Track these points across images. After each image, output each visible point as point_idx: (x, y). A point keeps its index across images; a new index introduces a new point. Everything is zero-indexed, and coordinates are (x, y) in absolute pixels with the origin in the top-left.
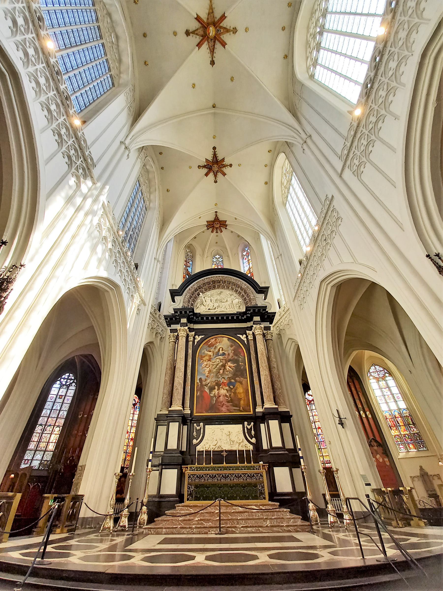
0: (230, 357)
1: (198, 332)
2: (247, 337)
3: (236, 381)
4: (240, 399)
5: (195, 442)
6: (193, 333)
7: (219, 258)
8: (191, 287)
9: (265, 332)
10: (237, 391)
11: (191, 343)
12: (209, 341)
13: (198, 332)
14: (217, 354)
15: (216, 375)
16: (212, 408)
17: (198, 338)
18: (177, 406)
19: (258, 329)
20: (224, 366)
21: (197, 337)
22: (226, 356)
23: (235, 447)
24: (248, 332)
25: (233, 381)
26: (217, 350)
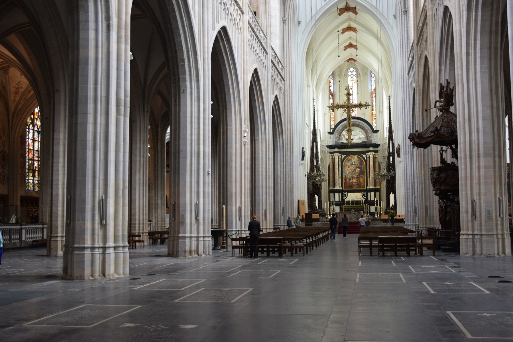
0: (358, 166)
1: (343, 153)
2: (366, 156)
3: (360, 176)
4: (361, 184)
5: (344, 198)
6: (341, 154)
7: (353, 71)
8: (339, 129)
9: (375, 153)
10: (360, 181)
11: (340, 159)
12: (348, 158)
13: (343, 153)
14: (352, 164)
15: (352, 174)
16: (351, 187)
17: (343, 156)
18: (337, 188)
19: (371, 154)
20: (355, 170)
21: (343, 156)
22: (356, 165)
23: (359, 200)
24: (366, 154)
25: (359, 176)
26: (352, 163)
